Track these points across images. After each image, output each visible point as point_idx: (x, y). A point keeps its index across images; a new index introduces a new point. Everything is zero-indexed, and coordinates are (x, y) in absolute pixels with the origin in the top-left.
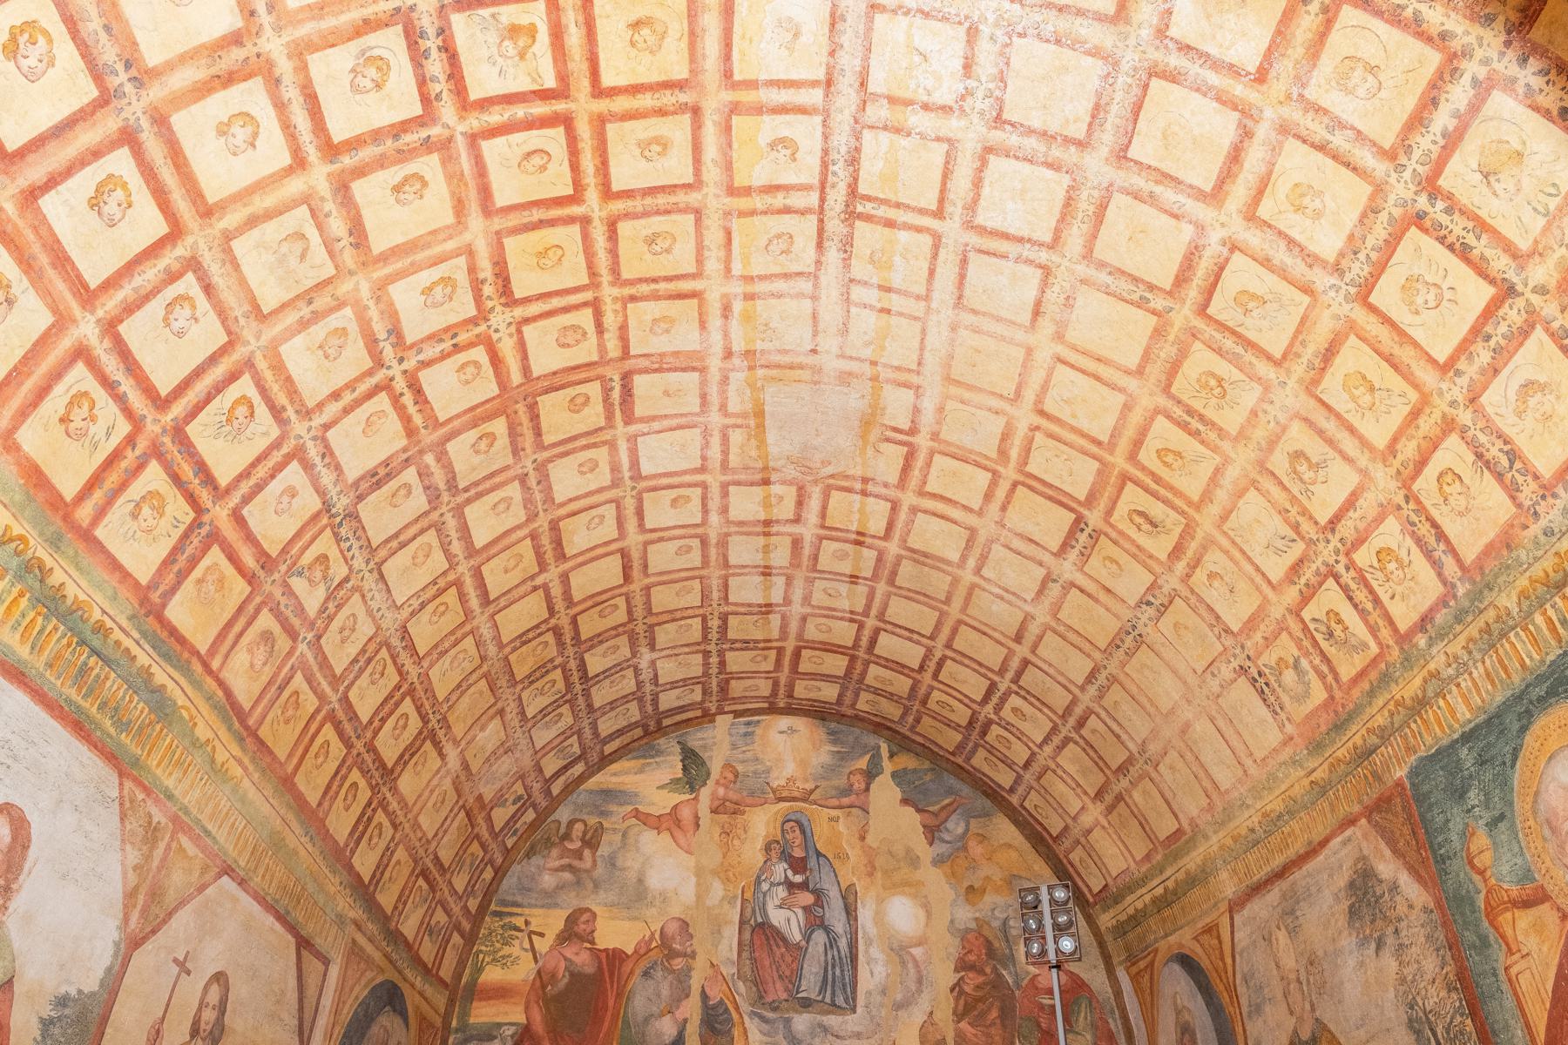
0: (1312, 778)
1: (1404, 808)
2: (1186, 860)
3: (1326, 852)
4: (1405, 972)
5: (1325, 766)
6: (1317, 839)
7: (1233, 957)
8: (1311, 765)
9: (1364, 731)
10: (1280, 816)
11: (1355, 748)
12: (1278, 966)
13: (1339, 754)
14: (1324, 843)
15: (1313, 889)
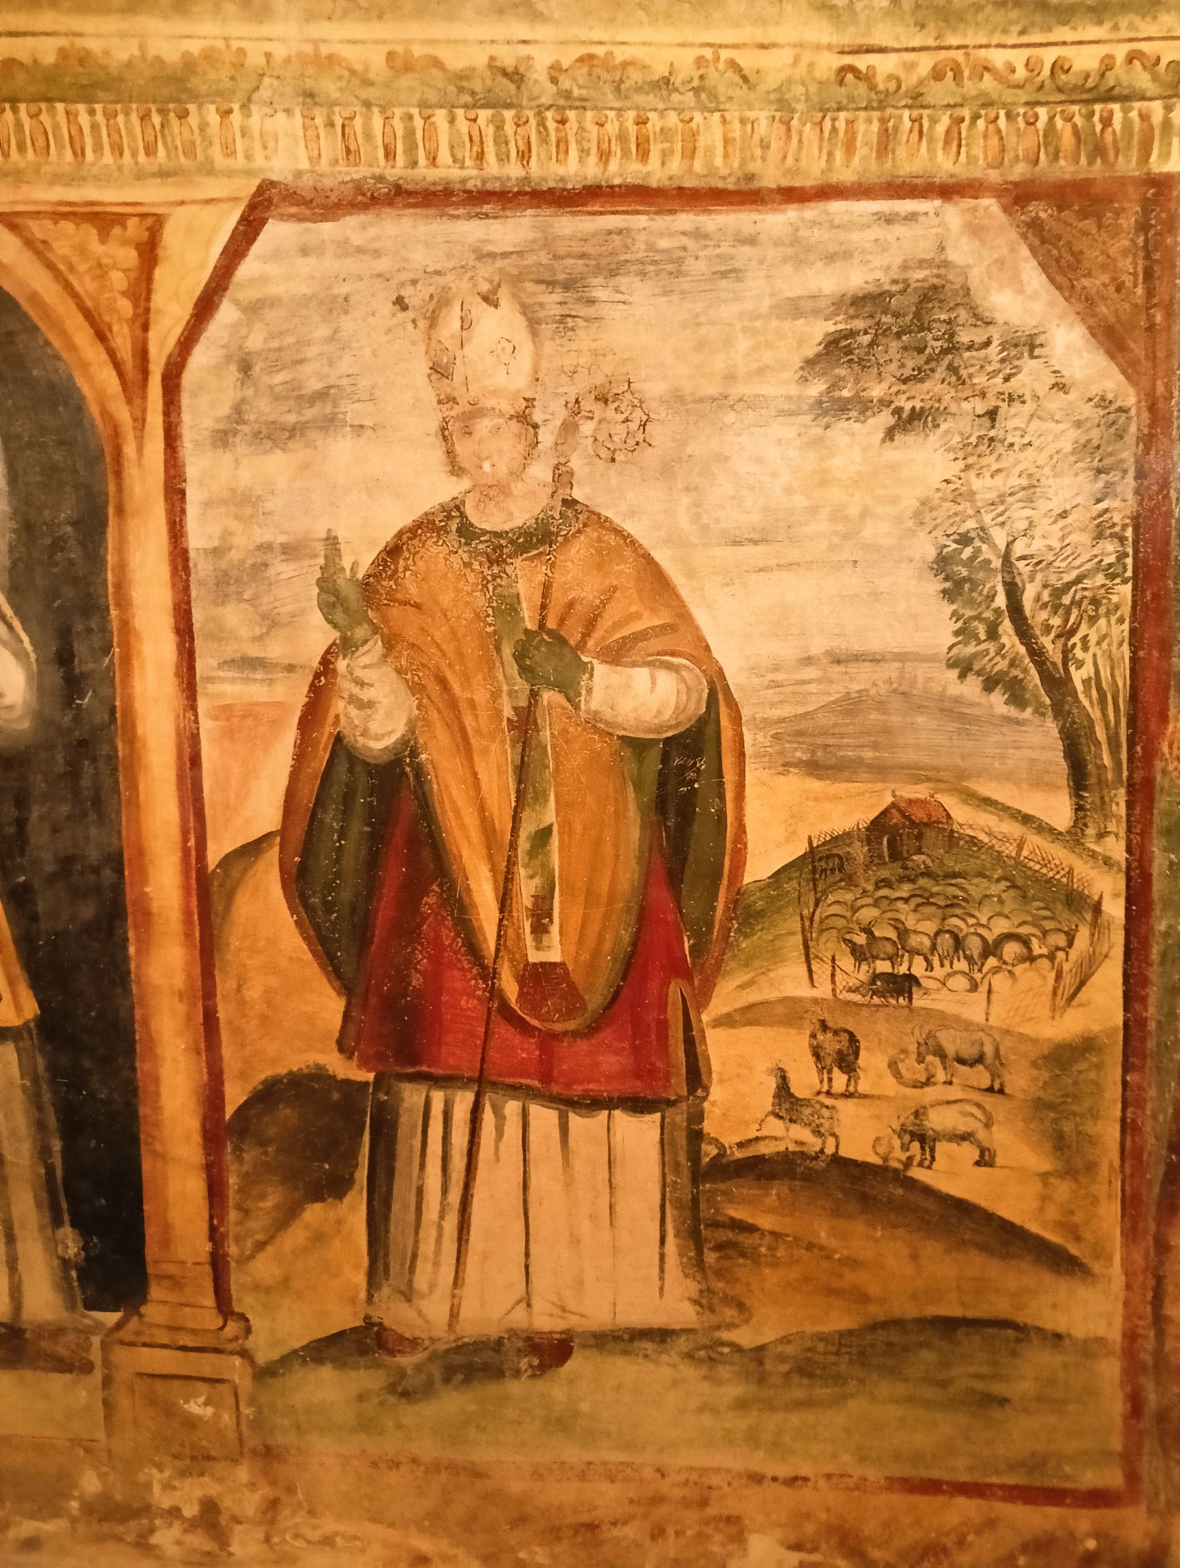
0: (862, 62)
1: (1143, 227)
2: (110, 24)
3: (811, 211)
4: (976, 484)
5: (926, 62)
6: (771, 176)
7: (205, 307)
8: (880, 37)
9: (1120, 52)
10: (665, 84)
11: (1058, 67)
12: (440, 371)
13: (998, 58)
14: (827, 192)
15: (697, 267)
